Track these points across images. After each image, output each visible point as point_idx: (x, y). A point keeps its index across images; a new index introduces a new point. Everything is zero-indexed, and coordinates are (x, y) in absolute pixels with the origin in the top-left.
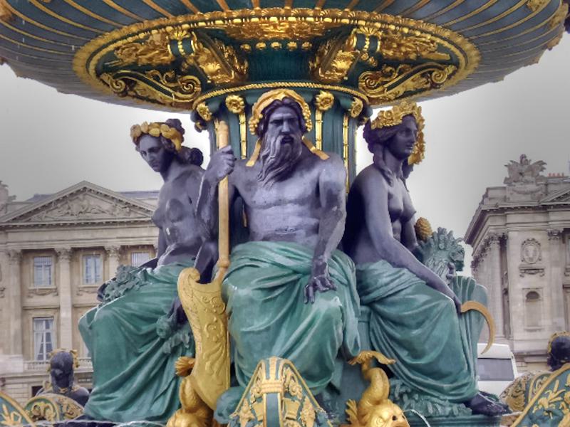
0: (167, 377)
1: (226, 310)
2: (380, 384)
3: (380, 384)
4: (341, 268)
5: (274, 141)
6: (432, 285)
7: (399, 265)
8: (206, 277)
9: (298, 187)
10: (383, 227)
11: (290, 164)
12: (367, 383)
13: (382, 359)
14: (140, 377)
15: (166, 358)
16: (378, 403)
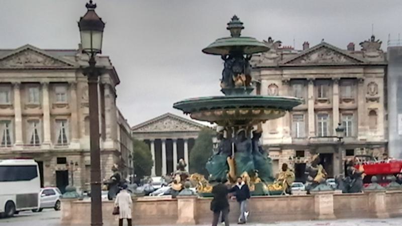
0: (223, 174)
1: (235, 164)
2: (257, 174)
3: (257, 174)
4: (251, 157)
5: (241, 137)
6: (264, 159)
7: (259, 156)
8: (231, 158)
9: (244, 143)
10: (257, 149)
11: (244, 139)
12: (255, 175)
13: (257, 171)
14: (220, 173)
15: (223, 171)
16: (256, 178)
